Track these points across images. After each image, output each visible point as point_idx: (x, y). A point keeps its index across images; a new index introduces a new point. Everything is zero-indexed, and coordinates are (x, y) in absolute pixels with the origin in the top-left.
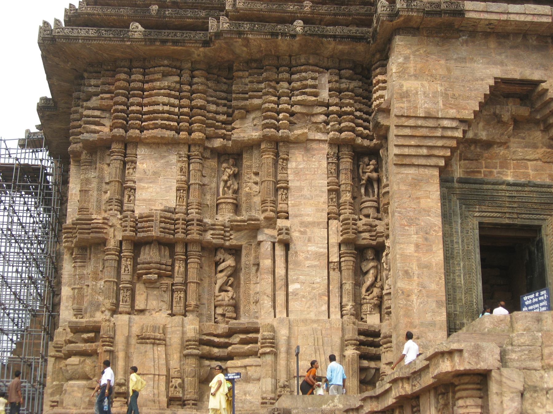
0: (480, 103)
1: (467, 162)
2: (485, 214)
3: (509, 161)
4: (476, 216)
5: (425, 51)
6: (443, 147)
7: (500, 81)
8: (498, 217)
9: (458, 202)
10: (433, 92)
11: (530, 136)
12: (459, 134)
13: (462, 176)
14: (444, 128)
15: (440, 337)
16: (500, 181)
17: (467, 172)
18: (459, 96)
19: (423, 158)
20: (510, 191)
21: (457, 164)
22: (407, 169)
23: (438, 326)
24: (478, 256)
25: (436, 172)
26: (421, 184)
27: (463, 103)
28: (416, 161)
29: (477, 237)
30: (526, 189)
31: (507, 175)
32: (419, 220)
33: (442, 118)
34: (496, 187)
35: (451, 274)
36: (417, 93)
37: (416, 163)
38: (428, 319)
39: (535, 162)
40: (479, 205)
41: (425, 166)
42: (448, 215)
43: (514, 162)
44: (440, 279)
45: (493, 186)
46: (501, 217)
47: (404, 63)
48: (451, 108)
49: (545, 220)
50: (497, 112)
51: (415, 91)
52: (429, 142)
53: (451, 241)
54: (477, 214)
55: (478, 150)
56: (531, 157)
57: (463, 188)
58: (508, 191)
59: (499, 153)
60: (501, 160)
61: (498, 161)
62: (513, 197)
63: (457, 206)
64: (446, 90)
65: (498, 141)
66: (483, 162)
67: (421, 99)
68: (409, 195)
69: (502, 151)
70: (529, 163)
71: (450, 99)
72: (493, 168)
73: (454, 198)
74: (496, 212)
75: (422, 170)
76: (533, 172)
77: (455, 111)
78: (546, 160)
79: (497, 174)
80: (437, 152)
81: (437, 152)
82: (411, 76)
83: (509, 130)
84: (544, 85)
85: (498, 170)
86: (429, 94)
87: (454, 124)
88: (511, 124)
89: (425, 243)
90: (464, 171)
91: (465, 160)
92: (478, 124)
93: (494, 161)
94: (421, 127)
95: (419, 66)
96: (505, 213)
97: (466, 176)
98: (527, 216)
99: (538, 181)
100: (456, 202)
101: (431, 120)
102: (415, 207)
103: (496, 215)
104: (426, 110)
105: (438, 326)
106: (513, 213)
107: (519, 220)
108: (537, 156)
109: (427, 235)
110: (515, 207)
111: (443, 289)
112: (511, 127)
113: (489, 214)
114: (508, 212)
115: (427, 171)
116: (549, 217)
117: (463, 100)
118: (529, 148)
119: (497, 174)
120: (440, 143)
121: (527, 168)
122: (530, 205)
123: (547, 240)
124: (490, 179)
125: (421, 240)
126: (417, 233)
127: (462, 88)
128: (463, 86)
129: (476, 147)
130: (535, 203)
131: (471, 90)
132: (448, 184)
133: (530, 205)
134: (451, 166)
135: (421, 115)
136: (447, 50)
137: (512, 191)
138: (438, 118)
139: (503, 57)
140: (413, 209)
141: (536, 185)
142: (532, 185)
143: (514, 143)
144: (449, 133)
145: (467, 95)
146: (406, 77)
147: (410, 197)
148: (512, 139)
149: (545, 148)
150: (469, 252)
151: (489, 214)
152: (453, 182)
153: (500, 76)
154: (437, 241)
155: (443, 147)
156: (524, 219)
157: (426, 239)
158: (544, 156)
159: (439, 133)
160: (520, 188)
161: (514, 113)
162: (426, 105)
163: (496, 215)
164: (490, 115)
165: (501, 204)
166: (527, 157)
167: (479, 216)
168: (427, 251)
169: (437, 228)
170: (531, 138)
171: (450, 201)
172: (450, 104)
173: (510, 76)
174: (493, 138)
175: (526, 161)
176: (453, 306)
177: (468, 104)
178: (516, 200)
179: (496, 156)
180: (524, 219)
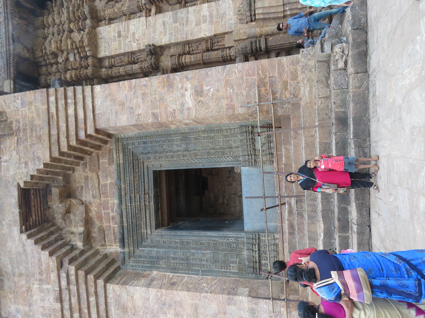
0: (43, 249)
1: (106, 239)
2: (148, 224)
3: (102, 202)
4: (151, 232)
5: (10, 294)
6: (86, 283)
7: (24, 227)
8: (150, 211)
9: (140, 248)
10: (40, 292)
11: (80, 182)
12: (72, 269)
13: (118, 245)
14: (68, 283)
15: (265, 306)
16: (119, 211)
17: (115, 239)
18: (39, 268)
19: (99, 300)
20: (126, 202)
21: (110, 249)
22: (110, 313)
23: (254, 306)
24: (184, 233)
25: (110, 287)
26: (122, 303)
27: (44, 266)
28: (102, 307)
29: (168, 232)
30: (123, 186)
31: (114, 204)
32: (153, 310)
33: (60, 287)
34: (124, 214)
35: (202, 263)
36: (43, 307)
37: (104, 306)
38: (247, 316)
39: (100, 178)
40: (141, 229)
41: (106, 297)
42: (151, 260)
43: (102, 196)
44: (206, 298)
45: (124, 216)
46: (150, 209)
47: (22, 314)
48: (50, 278)
49: (148, 167)
50: (60, 216)
51: (42, 309)
52: (84, 296)
53: (173, 260)
54: (149, 231)
55: (95, 230)
56: (96, 182)
57: (128, 244)
58: (126, 204)
59: (96, 211)
60: (102, 208)
61: (103, 212)
62: (130, 199)
63: (143, 250)
64: (36, 280)
65: (84, 214)
66: (105, 224)
67: (47, 304)
68: (133, 316)
69: (94, 209)
70: (102, 183)
71: (43, 277)
72: (109, 216)
73: (138, 252)
74: (146, 213)
75: (110, 300)
76: (109, 179)
77: (52, 275)
78: (97, 168)
79: (114, 213)
80: (92, 290)
81: (92, 290)
82: (30, 310)
83: (75, 203)
84: (22, 185)
85: (110, 211)
86: (42, 296)
87: (63, 275)
88: (70, 201)
89: (173, 307)
90: (115, 242)
91: (105, 242)
92: (72, 233)
93: (103, 215)
94: (70, 304)
95: (22, 302)
96: (145, 205)
97: (118, 240)
98: (146, 185)
99: (115, 176)
100: (140, 250)
101: (63, 296)
102: (142, 312)
103: (148, 214)
104: (55, 301)
105: (254, 306)
106: (144, 198)
107: (150, 192)
108: (95, 176)
109: (167, 304)
110: (140, 196)
111: (216, 296)
112: (73, 201)
113: (148, 221)
114: (145, 203)
115: (110, 295)
116: (145, 164)
117: (42, 265)
118: (88, 184)
119: (114, 213)
120: (83, 287)
121: (106, 185)
122: (136, 183)
123: (165, 167)
124: (118, 219)
125: (171, 311)
126: (165, 314)
127: (33, 265)
128: (31, 263)
129: (94, 232)
130: (134, 178)
131: (34, 257)
132: (127, 258)
133: (136, 183)
134: (111, 253)
135: (60, 306)
136: (7, 274)
137: (126, 199)
138: (60, 290)
139: (4, 223)
140: (145, 313)
141: (119, 178)
142: (119, 182)
143: (86, 197)
144: (73, 278)
145: (38, 261)
146: (31, 314)
147: (134, 315)
148: (84, 199)
149: (86, 170)
150: (182, 243)
151: (148, 221)
152: (124, 253)
153: (19, 228)
154: (171, 296)
155: (86, 283)
156: (149, 187)
157: (170, 306)
158: (93, 170)
159: (73, 288)
160: (123, 192)
161: (58, 203)
162: (51, 301)
163: (148, 214)
164: (65, 221)
165: (138, 209)
166: (97, 185)
167: (151, 230)
168: (181, 306)
169: (159, 294)
170: (81, 181)
171: (140, 256)
172: (47, 277)
173: (18, 218)
174: (81, 221)
175: (100, 186)
176: (231, 265)
177: (44, 261)
178: (133, 195)
179: (99, 214)
180: (149, 187)
